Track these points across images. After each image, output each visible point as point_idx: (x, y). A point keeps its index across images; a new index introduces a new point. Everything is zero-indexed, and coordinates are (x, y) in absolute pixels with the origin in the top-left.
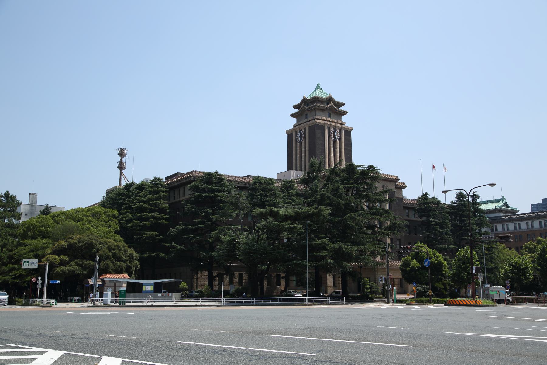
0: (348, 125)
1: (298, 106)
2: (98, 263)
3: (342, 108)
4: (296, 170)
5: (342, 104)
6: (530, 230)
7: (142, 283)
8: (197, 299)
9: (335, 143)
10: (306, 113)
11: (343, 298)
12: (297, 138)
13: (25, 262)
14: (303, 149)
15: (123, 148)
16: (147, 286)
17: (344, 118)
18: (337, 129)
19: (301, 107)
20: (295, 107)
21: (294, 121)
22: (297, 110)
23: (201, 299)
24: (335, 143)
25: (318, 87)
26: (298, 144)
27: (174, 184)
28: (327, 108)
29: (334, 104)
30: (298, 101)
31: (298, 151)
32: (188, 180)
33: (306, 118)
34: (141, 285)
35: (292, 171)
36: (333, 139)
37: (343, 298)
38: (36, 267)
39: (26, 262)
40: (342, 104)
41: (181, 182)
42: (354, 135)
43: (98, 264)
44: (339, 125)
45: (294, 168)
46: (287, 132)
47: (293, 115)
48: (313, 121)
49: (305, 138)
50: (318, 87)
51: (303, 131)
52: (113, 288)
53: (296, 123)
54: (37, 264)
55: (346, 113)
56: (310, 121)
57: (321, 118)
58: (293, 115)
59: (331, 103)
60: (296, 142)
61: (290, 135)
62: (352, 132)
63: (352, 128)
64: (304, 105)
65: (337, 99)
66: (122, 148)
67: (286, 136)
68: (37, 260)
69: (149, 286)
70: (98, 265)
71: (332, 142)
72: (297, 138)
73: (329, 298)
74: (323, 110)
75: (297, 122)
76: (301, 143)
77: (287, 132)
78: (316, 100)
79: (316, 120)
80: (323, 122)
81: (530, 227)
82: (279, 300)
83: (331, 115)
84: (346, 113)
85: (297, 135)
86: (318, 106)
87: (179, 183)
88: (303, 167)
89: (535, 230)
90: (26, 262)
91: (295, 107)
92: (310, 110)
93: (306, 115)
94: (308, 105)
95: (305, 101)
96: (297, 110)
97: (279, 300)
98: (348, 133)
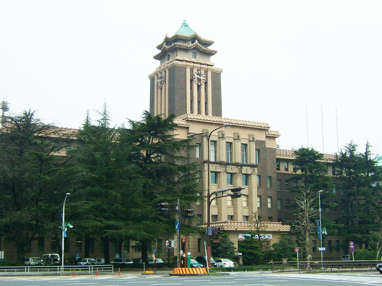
3: (211, 48)
9: (199, 87)
10: (169, 54)
11: (112, 266)
15: (5, 101)
17: (213, 59)
18: (201, 71)
24: (199, 87)
26: (159, 90)
30: (161, 41)
36: (197, 83)
37: (112, 266)
42: (223, 76)
57: (183, 58)
62: (222, 75)
63: (221, 69)
65: (204, 37)
66: (4, 101)
67: (149, 81)
73: (91, 267)
74: (186, 50)
76: (161, 89)
82: (58, 269)
83: (197, 56)
86: (179, 46)
91: (159, 47)
93: (169, 56)
97: (26, 269)
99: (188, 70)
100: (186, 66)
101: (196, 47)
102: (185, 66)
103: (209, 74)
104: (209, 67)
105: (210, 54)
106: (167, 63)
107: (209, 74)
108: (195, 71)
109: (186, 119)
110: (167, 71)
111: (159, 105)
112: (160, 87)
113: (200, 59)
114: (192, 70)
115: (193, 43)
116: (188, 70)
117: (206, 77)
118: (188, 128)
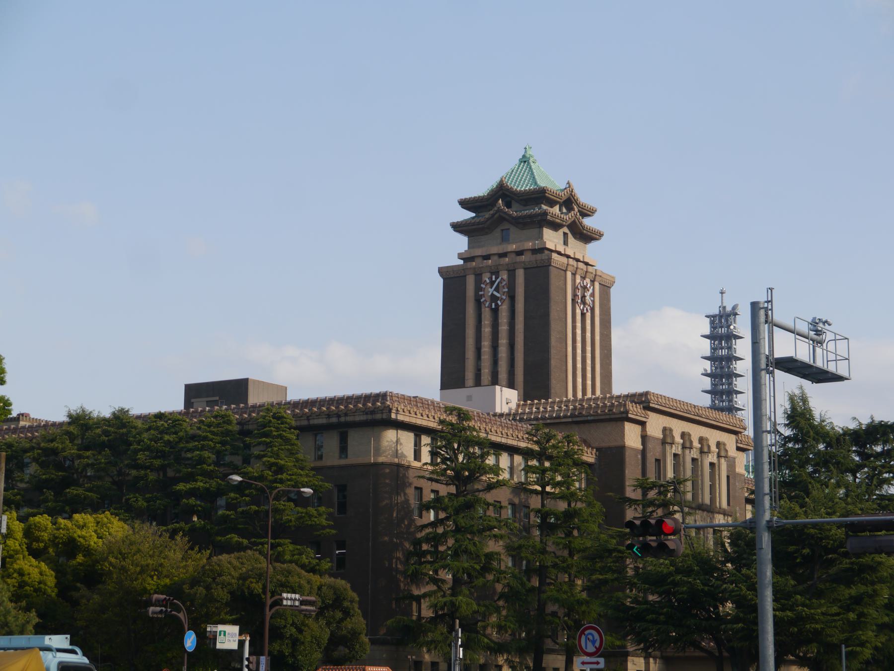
1: (476, 204)
3: (587, 222)
12: (481, 293)
13: (220, 632)
19: (496, 209)
20: (466, 204)
21: (461, 243)
22: (468, 215)
24: (583, 315)
27: (308, 419)
29: (579, 211)
30: (481, 188)
31: (487, 330)
32: (378, 416)
33: (505, 239)
35: (498, 388)
38: (234, 646)
39: (222, 633)
41: (342, 419)
43: (461, 646)
46: (444, 272)
47: (458, 227)
49: (512, 298)
51: (505, 277)
53: (467, 249)
54: (237, 638)
56: (520, 253)
58: (458, 227)
59: (573, 209)
62: (612, 290)
65: (584, 197)
67: (442, 280)
68: (235, 629)
70: (461, 649)
72: (481, 293)
74: (555, 226)
75: (469, 248)
76: (495, 312)
77: (443, 271)
78: (540, 196)
79: (554, 255)
80: (564, 260)
85: (483, 286)
87: (334, 420)
88: (503, 375)
90: (222, 633)
91: (466, 204)
94: (509, 205)
95: (502, 192)
96: (468, 215)
98: (606, 288)
99: (569, 274)
100: (567, 267)
101: (574, 221)
102: (566, 265)
103: (597, 285)
105: (587, 236)
107: (597, 285)
108: (578, 280)
109: (645, 405)
110: (520, 274)
111: (486, 344)
113: (575, 248)
114: (574, 274)
115: (560, 210)
116: (569, 274)
117: (593, 295)
118: (643, 424)
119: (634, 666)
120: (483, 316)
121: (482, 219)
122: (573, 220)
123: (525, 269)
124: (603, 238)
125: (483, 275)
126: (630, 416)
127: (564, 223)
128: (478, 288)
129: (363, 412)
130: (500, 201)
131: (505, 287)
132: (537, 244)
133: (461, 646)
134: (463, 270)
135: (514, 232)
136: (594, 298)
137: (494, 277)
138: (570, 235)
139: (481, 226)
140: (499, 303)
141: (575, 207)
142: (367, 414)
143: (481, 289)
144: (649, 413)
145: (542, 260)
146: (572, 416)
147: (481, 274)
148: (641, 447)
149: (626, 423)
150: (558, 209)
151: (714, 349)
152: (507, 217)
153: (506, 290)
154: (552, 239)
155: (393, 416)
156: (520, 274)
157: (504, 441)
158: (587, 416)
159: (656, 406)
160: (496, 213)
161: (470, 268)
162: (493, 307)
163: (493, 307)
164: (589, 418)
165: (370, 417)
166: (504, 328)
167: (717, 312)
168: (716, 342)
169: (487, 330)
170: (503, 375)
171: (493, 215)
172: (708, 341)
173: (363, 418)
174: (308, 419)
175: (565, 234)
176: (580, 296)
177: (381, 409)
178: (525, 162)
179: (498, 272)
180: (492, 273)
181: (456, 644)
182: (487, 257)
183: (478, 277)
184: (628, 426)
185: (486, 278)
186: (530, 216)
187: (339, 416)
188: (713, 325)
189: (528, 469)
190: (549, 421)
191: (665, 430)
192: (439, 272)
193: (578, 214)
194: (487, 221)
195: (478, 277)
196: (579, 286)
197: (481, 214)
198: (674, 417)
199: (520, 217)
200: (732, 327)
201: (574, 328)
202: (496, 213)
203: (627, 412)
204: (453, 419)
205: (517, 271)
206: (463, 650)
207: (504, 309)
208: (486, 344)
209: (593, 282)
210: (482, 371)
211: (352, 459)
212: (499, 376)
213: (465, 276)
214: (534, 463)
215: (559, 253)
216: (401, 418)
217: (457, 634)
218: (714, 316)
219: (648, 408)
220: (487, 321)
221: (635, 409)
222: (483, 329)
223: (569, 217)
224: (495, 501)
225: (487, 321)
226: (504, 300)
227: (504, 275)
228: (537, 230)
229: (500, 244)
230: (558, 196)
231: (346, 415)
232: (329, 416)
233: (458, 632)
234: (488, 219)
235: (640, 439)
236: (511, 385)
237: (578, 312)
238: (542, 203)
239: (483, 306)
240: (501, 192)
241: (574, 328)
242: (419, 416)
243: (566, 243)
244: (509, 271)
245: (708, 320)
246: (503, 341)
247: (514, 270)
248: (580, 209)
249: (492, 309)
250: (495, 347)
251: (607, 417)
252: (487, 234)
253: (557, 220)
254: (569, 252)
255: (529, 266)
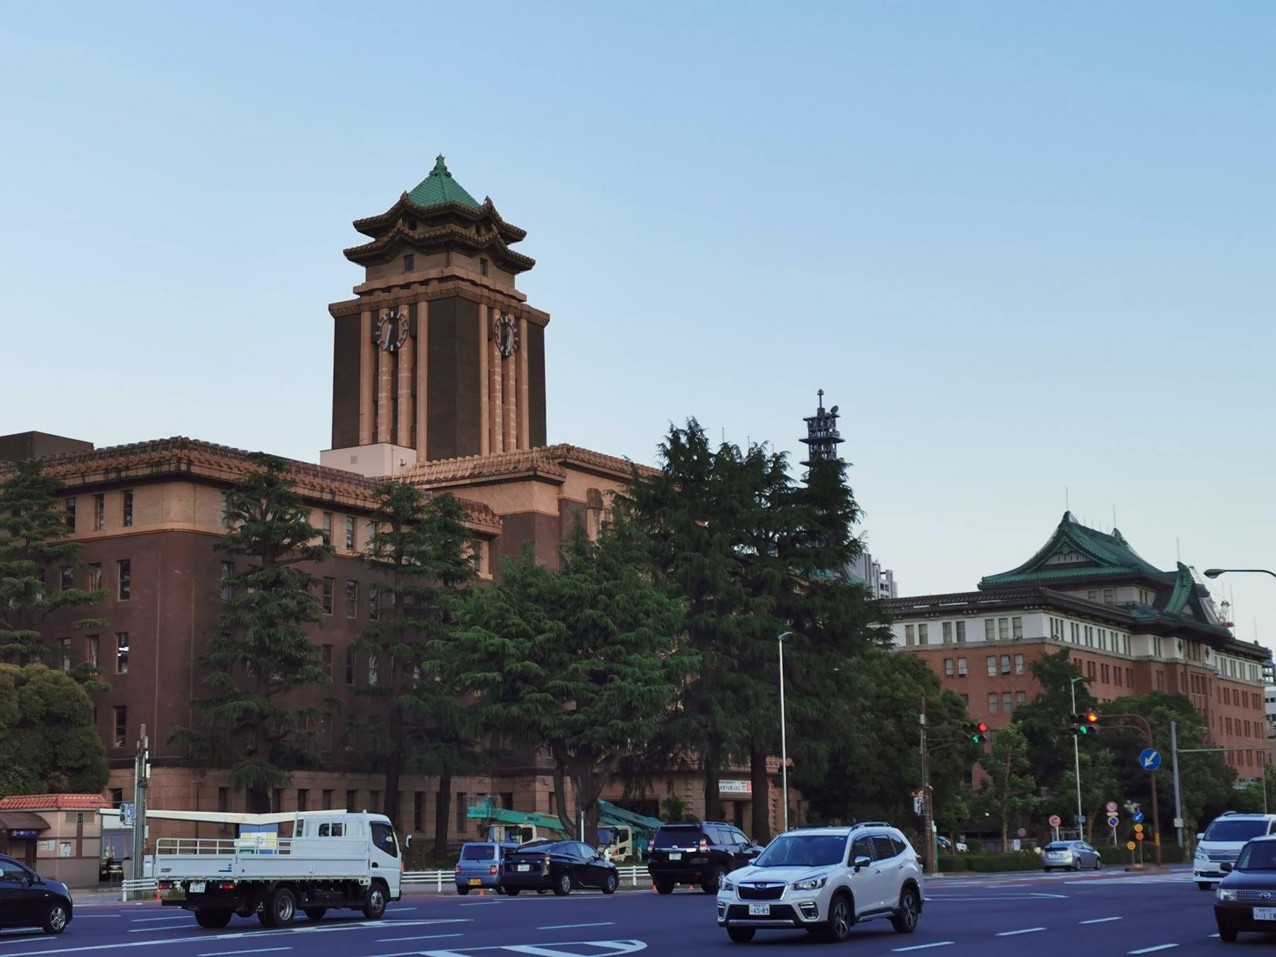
0: (534, 302)
2: (147, 757)
3: (513, 247)
4: (394, 440)
5: (518, 235)
6: (915, 649)
7: (237, 825)
8: (437, 874)
10: (409, 253)
12: (377, 333)
14: (404, 375)
16: (254, 835)
17: (522, 282)
19: (395, 230)
20: (362, 226)
21: (358, 275)
22: (366, 240)
23: (442, 874)
24: (504, 357)
25: (440, 172)
26: (384, 357)
27: (83, 476)
28: (482, 244)
30: (381, 206)
31: (385, 379)
32: (165, 468)
33: (409, 267)
34: (236, 830)
36: (502, 348)
40: (518, 235)
41: (123, 474)
43: (147, 761)
44: (514, 303)
45: (365, 434)
46: (335, 310)
47: (354, 255)
48: (450, 285)
49: (414, 338)
50: (440, 172)
52: (75, 842)
53: (364, 281)
55: (526, 264)
56: (426, 282)
58: (354, 255)
59: (491, 230)
60: (375, 345)
61: (345, 317)
62: (548, 331)
64: (403, 224)
65: (508, 216)
67: (333, 320)
69: (263, 835)
70: (148, 765)
71: (498, 361)
72: (377, 333)
74: (469, 250)
76: (395, 355)
77: (335, 310)
79: (462, 284)
81: (917, 642)
84: (525, 264)
85: (380, 324)
87: (113, 475)
88: (403, 434)
89: (929, 648)
91: (362, 226)
92: (429, 247)
94: (413, 227)
95: (405, 210)
96: (366, 240)
99: (484, 309)
103: (524, 324)
104: (514, 303)
106: (395, 276)
107: (524, 324)
108: (497, 316)
109: (560, 460)
110: (423, 308)
111: (384, 396)
112: (389, 346)
113: (494, 279)
114: (491, 310)
115: (478, 232)
116: (484, 309)
119: (545, 787)
120: (380, 361)
121: (380, 244)
122: (491, 243)
123: (429, 302)
124: (534, 268)
125: (380, 311)
126: (538, 473)
127: (480, 247)
128: (375, 328)
129: (147, 463)
130: (401, 221)
131: (405, 324)
132: (447, 273)
133: (147, 761)
134: (358, 305)
135: (419, 259)
136: (519, 338)
137: (392, 313)
138: (490, 263)
139: (379, 252)
140: (399, 344)
141: (495, 228)
142: (151, 466)
143: (378, 328)
144: (567, 470)
145: (448, 290)
146: (471, 476)
147: (378, 310)
148: (557, 513)
149: (534, 482)
150: (474, 232)
151: (812, 454)
152: (409, 240)
153: (406, 328)
154: (464, 267)
155: (183, 467)
156: (423, 308)
157: (359, 503)
158: (489, 476)
159: (576, 462)
160: (396, 236)
161: (366, 304)
162: (392, 349)
163: (392, 349)
164: (491, 478)
165: (155, 470)
166: (404, 375)
167: (815, 414)
168: (815, 447)
169: (385, 379)
170: (403, 434)
171: (393, 237)
172: (807, 445)
173: (147, 471)
174: (83, 476)
175: (483, 262)
176: (499, 335)
177: (167, 458)
178: (436, 175)
179: (398, 307)
180: (391, 309)
181: (141, 759)
182: (388, 289)
183: (375, 313)
184: (536, 487)
185: (383, 314)
186: (435, 238)
187: (118, 470)
188: (811, 430)
189: (379, 539)
190: (444, 484)
191: (590, 491)
192: (330, 309)
193: (499, 236)
194: (386, 246)
195: (375, 313)
196: (498, 323)
197: (380, 239)
198: (591, 474)
199: (424, 239)
200: (831, 430)
201: (491, 375)
202: (396, 236)
203: (535, 470)
204: (263, 470)
205: (419, 305)
206: (151, 767)
207: (404, 351)
208: (384, 396)
209: (518, 319)
210: (379, 429)
211: (139, 526)
212: (399, 435)
213: (360, 314)
214: (388, 529)
215: (473, 283)
216: (195, 470)
217: (142, 745)
218: (812, 419)
219: (565, 464)
220: (385, 368)
221: (547, 466)
222: (380, 378)
223: (485, 237)
224: (325, 577)
225: (385, 368)
226: (405, 340)
227: (404, 311)
228: (442, 256)
229: (403, 274)
230: (472, 213)
231: (127, 468)
232: (107, 471)
233: (142, 741)
234: (387, 243)
235: (556, 503)
236: (413, 445)
237: (497, 354)
238: (451, 222)
239: (380, 350)
240: (403, 210)
241: (491, 375)
242: (225, 468)
243: (484, 273)
244: (410, 305)
245: (806, 423)
246: (404, 391)
247: (416, 304)
248: (503, 231)
249: (390, 353)
250: (394, 399)
251: (512, 476)
252: (388, 262)
253: (469, 242)
254: (485, 281)
255: (433, 298)
